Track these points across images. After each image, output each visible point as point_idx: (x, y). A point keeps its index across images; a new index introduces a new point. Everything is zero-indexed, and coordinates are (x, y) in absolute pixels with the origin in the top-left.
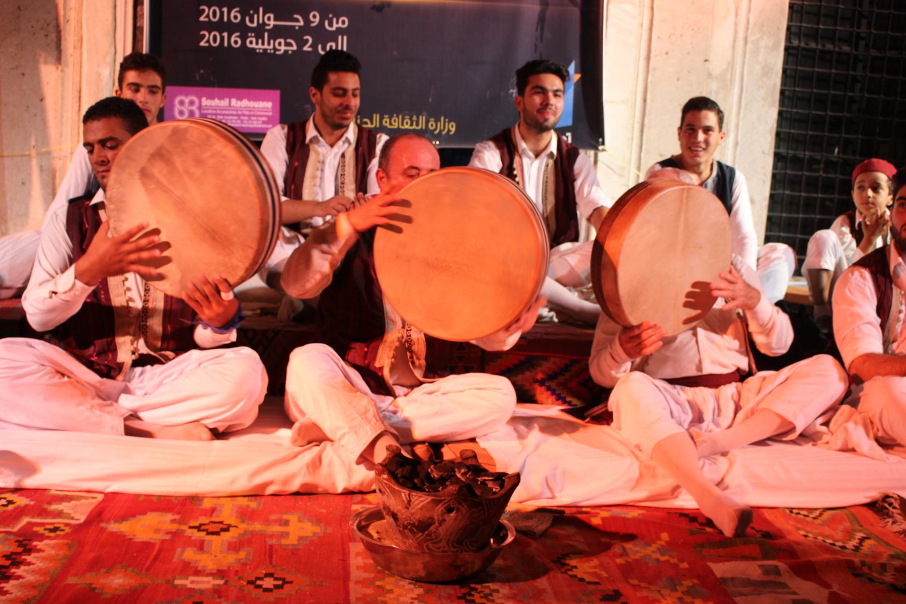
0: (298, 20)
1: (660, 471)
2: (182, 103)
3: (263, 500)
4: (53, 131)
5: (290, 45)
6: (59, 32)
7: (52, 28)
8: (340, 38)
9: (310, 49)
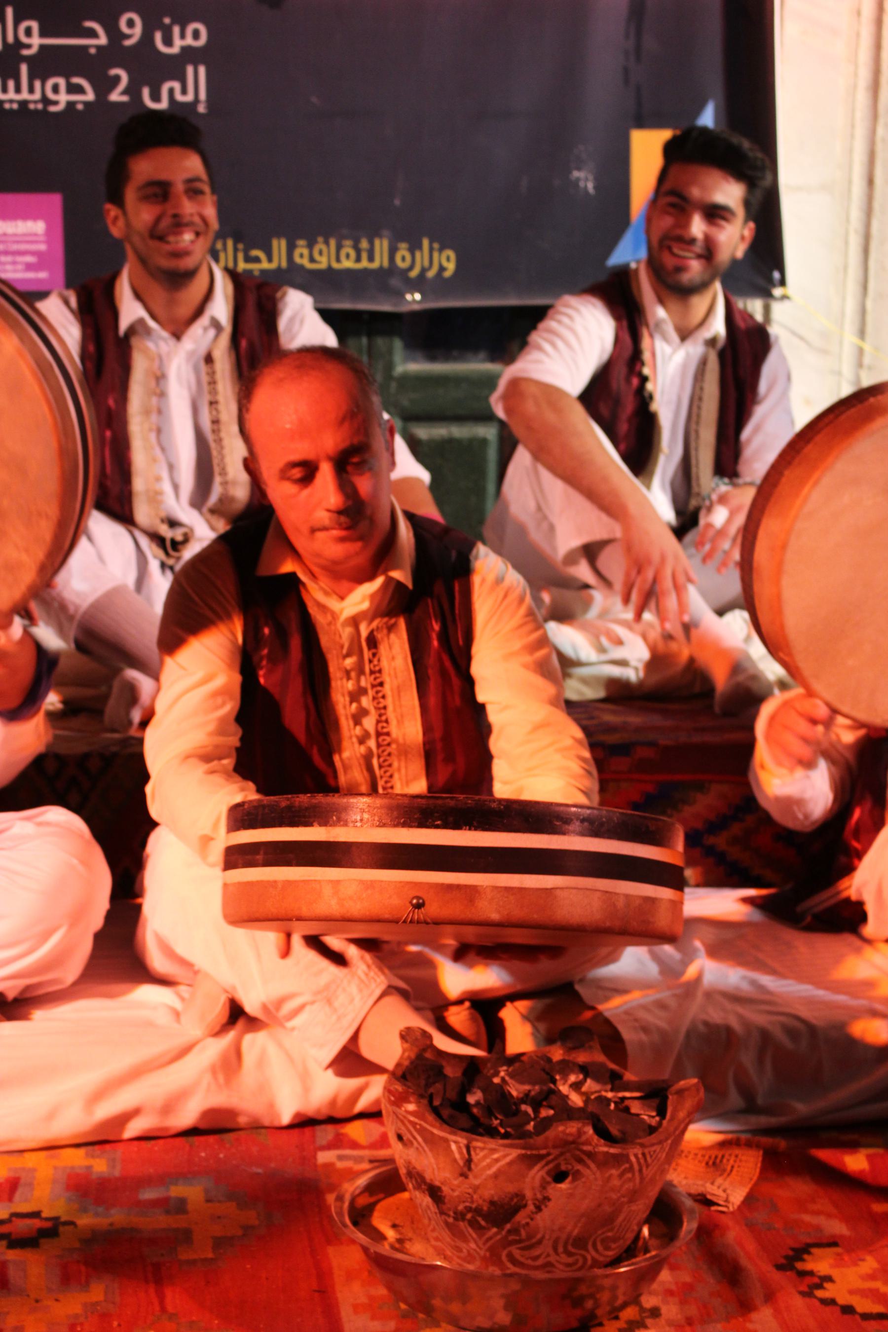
0: (93, 34)
3: (119, 1152)
5: (79, 90)
8: (190, 70)
9: (125, 98)
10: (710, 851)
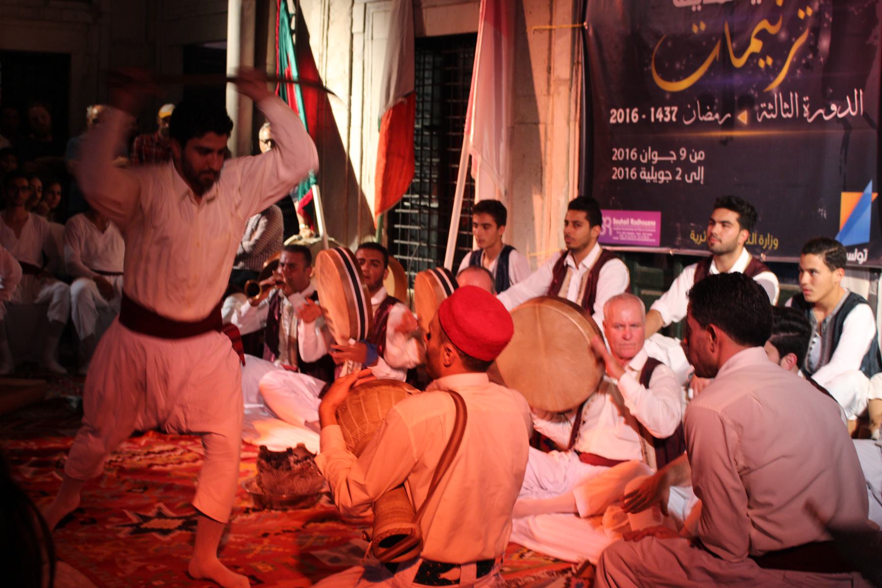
0: (672, 156)
4: (538, 242)
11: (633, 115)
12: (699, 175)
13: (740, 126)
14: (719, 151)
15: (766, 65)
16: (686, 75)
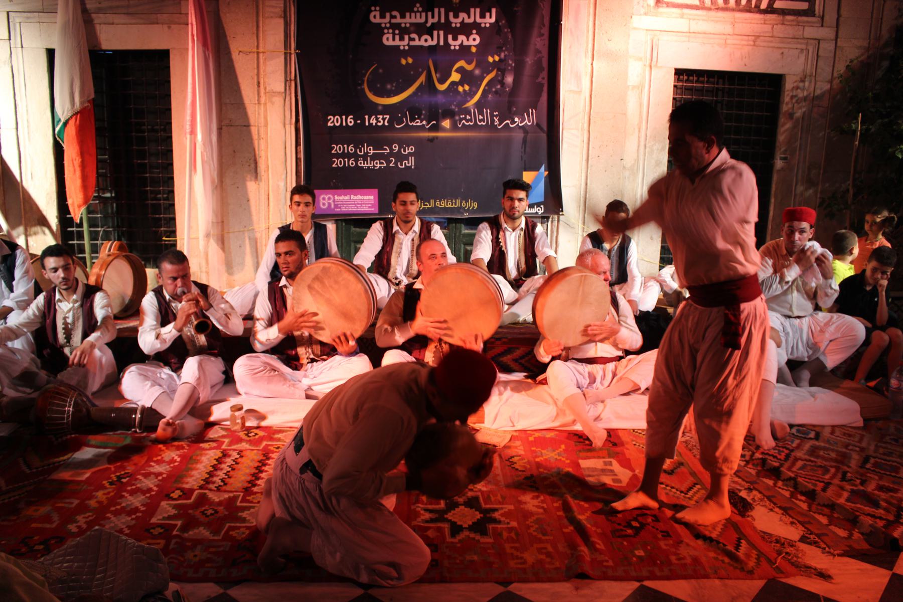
1: (568, 412)
2: (324, 199)
4: (255, 218)
6: (256, 163)
7: (252, 161)
10: (520, 364)
11: (349, 120)
12: (411, 162)
13: (444, 130)
14: (424, 148)
15: (464, 90)
16: (396, 93)
